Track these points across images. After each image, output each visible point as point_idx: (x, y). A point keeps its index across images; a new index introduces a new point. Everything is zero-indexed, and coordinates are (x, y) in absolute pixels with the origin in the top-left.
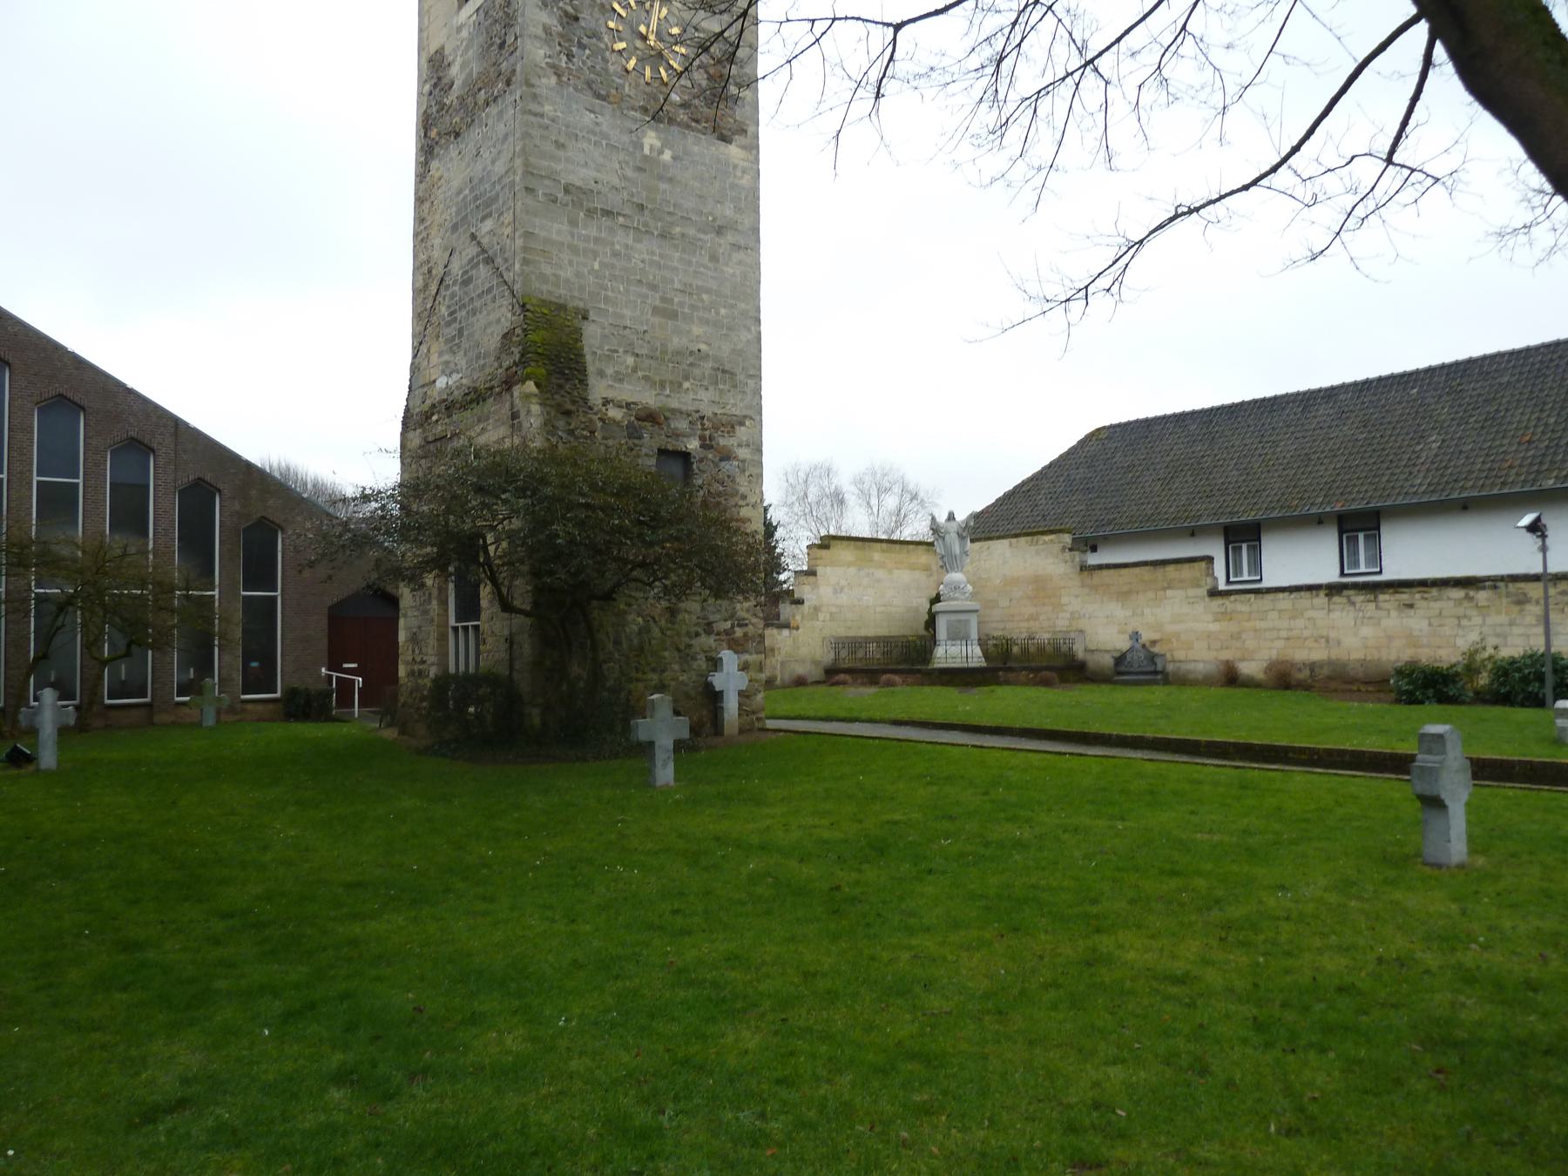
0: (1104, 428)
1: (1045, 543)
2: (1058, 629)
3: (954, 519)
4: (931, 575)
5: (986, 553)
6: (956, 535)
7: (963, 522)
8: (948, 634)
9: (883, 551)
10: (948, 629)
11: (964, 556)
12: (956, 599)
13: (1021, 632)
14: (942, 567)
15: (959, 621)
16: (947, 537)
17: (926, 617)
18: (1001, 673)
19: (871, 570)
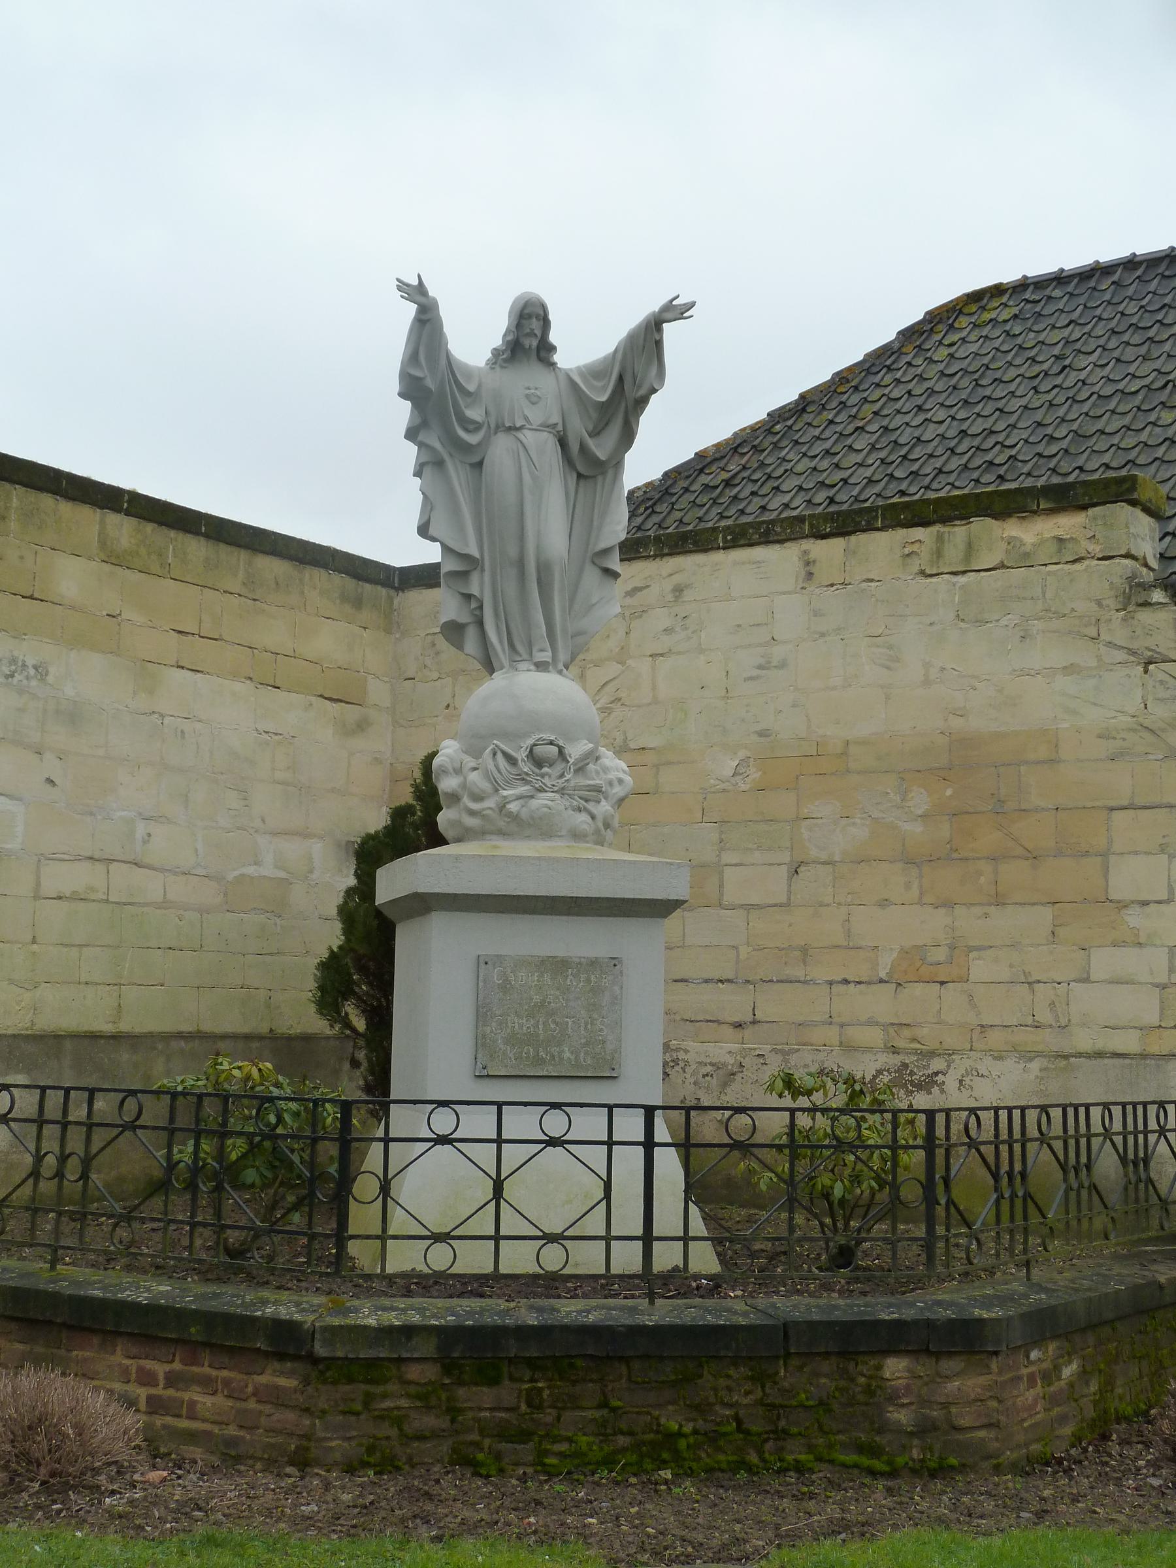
0: (997, 290)
1: (1024, 559)
2: (1084, 1041)
3: (545, 351)
4: (362, 726)
5: (660, 619)
6: (549, 443)
7: (595, 372)
8: (482, 1043)
9: (114, 558)
10: (482, 1014)
11: (591, 576)
12: (539, 827)
13: (849, 1048)
14: (454, 631)
15: (558, 966)
16: (500, 451)
17: (331, 936)
18: (895, 1368)
19: (30, 651)
